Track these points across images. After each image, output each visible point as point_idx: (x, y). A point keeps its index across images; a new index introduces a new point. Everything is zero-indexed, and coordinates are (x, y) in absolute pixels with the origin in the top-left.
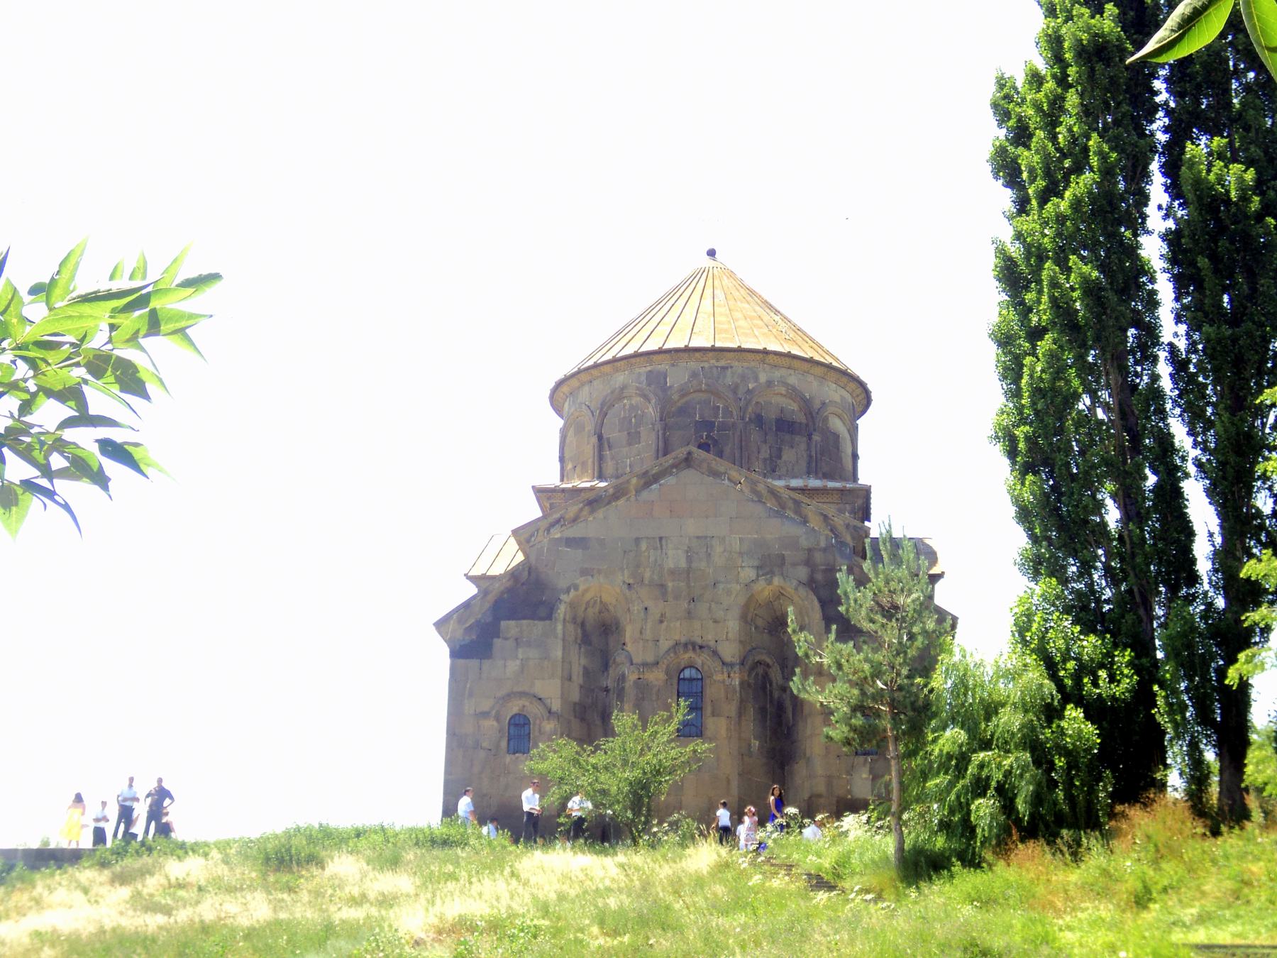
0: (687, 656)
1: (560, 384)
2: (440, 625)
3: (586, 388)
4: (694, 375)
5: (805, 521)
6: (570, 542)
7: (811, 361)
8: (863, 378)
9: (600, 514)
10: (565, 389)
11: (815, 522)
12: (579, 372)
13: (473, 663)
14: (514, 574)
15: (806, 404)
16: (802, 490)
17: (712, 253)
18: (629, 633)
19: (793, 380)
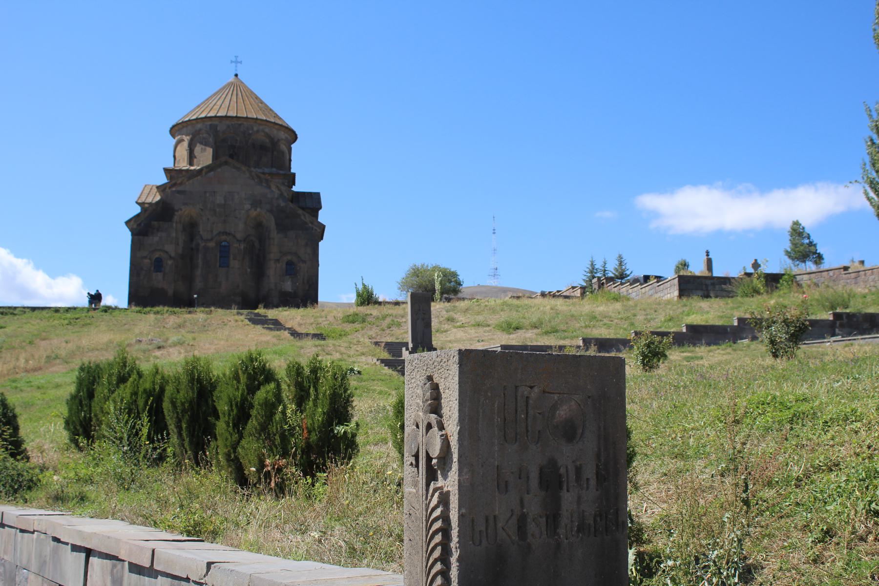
0: (224, 237)
1: (173, 127)
2: (127, 223)
3: (185, 129)
4: (228, 127)
5: (269, 187)
6: (179, 192)
7: (275, 123)
8: (295, 129)
9: (191, 181)
10: (176, 128)
11: (274, 188)
12: (183, 122)
13: (141, 237)
14: (158, 203)
15: (271, 139)
16: (270, 174)
17: (236, 75)
18: (201, 228)
19: (267, 130)
